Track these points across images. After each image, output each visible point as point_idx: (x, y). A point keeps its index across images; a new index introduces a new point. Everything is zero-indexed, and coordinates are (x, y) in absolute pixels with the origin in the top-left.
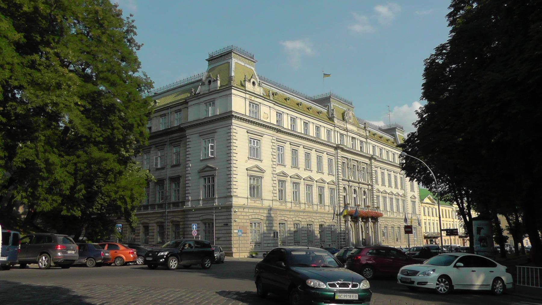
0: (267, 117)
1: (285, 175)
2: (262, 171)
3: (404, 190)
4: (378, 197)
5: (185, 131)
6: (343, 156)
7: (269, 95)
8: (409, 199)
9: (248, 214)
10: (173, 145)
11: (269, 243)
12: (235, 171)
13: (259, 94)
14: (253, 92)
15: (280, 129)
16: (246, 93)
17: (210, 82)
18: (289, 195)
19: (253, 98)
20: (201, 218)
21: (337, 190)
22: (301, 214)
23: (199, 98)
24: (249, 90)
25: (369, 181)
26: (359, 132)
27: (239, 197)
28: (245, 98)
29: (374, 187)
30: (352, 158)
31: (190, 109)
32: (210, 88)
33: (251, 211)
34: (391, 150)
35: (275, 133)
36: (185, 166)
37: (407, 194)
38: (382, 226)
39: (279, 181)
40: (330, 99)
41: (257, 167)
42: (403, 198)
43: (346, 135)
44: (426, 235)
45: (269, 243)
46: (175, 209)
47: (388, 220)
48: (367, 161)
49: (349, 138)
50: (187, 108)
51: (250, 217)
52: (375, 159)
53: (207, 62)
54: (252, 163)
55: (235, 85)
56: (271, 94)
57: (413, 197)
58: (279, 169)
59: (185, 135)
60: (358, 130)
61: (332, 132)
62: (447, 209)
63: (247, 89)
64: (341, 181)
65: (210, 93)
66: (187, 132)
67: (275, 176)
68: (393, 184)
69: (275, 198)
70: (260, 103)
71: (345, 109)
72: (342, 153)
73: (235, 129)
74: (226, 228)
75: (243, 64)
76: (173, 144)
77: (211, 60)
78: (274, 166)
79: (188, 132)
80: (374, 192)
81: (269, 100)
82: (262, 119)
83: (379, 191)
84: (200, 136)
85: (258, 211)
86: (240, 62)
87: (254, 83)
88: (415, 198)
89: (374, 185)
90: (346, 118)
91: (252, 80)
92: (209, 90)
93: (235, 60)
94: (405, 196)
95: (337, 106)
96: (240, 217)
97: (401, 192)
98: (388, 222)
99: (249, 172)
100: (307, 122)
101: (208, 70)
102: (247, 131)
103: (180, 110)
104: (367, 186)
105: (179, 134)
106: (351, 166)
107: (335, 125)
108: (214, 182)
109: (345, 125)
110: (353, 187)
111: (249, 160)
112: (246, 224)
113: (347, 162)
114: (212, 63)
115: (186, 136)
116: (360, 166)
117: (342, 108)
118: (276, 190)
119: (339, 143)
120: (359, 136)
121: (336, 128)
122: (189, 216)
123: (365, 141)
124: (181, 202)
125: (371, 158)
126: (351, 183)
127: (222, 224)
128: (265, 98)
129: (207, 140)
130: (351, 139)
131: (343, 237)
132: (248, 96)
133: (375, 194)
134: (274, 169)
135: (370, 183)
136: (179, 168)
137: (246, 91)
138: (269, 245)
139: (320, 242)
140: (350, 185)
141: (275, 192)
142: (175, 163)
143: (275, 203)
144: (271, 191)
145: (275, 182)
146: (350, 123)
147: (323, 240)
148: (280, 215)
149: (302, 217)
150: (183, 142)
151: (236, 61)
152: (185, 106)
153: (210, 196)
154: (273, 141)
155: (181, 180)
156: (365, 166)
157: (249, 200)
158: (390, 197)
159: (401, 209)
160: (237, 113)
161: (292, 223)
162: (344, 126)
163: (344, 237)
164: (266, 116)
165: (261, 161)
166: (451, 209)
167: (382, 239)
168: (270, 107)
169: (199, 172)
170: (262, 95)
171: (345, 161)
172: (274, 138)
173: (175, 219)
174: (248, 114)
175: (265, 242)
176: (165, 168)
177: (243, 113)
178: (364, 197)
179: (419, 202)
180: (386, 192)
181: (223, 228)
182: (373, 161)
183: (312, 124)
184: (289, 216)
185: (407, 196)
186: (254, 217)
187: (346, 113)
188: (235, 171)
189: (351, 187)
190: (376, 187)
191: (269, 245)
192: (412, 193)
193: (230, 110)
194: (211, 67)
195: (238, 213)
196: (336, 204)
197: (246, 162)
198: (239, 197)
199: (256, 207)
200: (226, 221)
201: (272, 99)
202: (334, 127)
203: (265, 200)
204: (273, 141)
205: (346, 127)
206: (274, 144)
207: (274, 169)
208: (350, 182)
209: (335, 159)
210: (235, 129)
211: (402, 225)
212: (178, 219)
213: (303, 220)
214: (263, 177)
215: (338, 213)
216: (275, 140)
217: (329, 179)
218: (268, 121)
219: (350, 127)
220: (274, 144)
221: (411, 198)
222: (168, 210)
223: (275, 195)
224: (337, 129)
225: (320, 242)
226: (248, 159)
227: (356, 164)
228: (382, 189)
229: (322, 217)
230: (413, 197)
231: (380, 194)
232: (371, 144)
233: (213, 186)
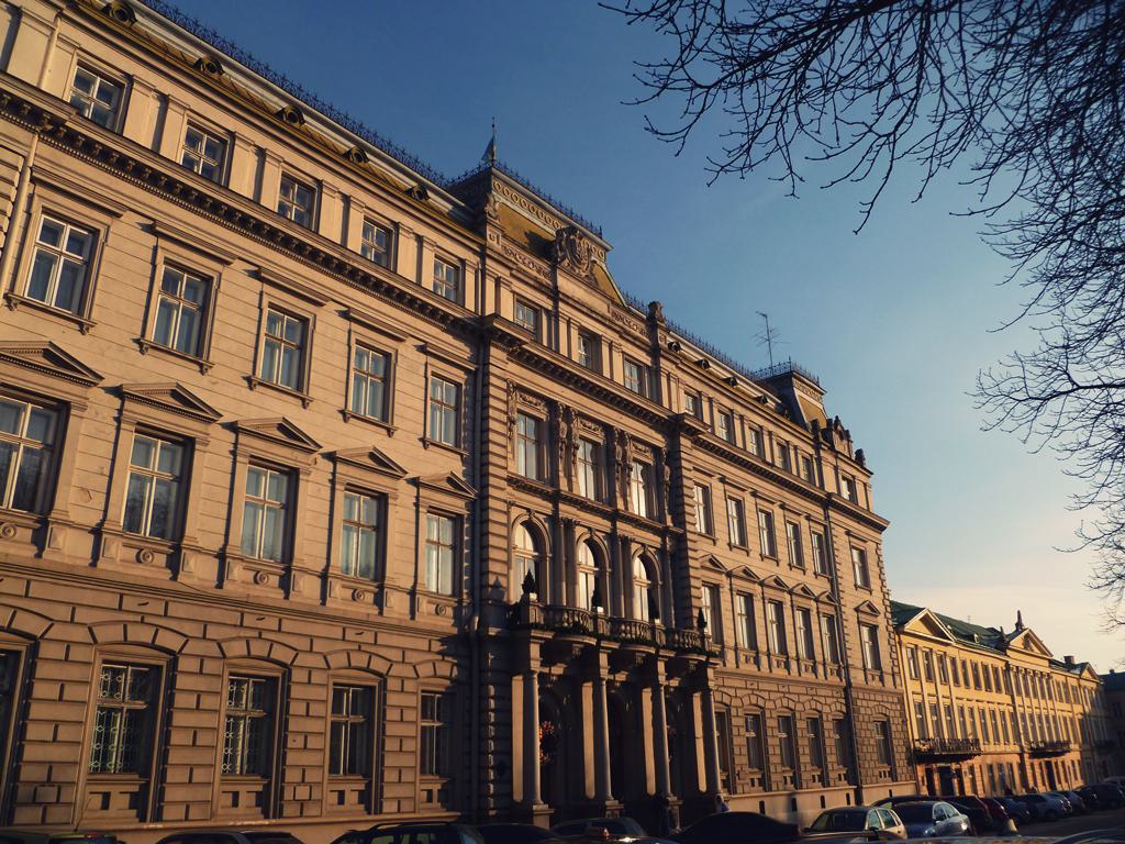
25: (669, 518)
29: (690, 544)
38: (733, 712)
40: (490, 180)
42: (830, 611)
43: (547, 311)
52: (692, 433)
62: (989, 662)
64: (503, 484)
68: (783, 551)
72: (513, 367)
80: (691, 562)
83: (715, 564)
88: (874, 611)
89: (689, 536)
95: (526, 215)
104: (659, 539)
109: (545, 275)
120: (617, 336)
121: (488, 261)
125: (673, 427)
133: (698, 574)
135: (669, 523)
146: (577, 278)
166: (1000, 665)
180: (748, 575)
190: (699, 550)
192: (863, 596)
219: (565, 284)
221: (857, 610)
228: (732, 560)
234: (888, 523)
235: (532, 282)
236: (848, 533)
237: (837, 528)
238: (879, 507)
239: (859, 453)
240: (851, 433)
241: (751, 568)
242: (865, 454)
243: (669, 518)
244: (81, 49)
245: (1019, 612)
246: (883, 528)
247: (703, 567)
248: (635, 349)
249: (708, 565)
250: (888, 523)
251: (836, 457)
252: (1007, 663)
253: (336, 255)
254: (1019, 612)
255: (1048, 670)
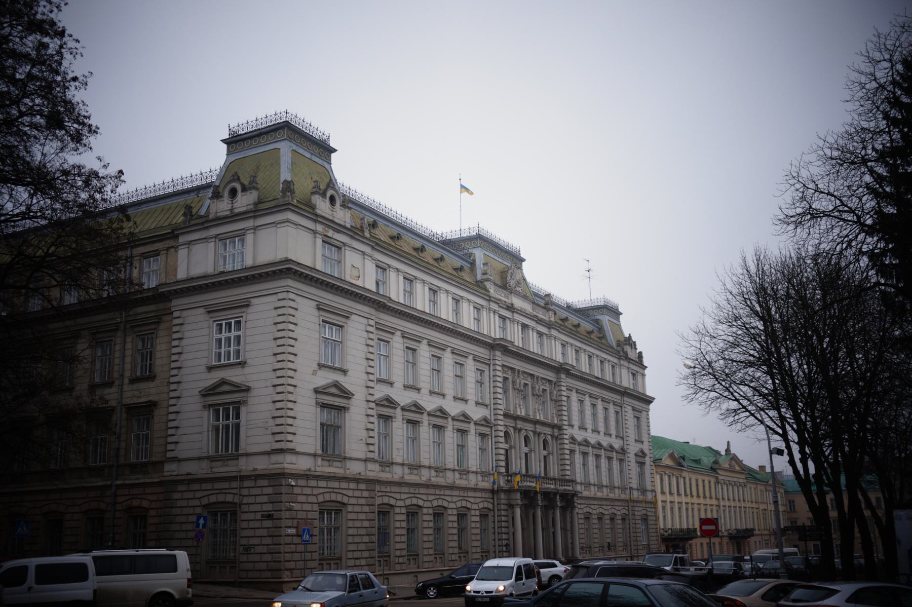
0: (357, 275)
1: (389, 402)
2: (346, 395)
3: (622, 438)
4: (572, 452)
5: (170, 301)
6: (505, 364)
7: (362, 227)
8: (632, 458)
9: (316, 491)
10: (135, 333)
11: (358, 559)
12: (292, 393)
13: (342, 223)
14: (331, 218)
15: (384, 303)
16: (316, 221)
17: (233, 193)
18: (398, 449)
19: (330, 233)
20: (205, 501)
21: (493, 439)
22: (422, 491)
23: (207, 228)
24: (324, 214)
25: (555, 419)
26: (535, 313)
27: (298, 453)
28: (314, 232)
30: (522, 369)
31: (182, 253)
32: (235, 205)
33: (322, 484)
34: (597, 352)
35: (373, 311)
36: (167, 380)
37: (628, 447)
39: (380, 416)
41: (336, 385)
42: (621, 457)
43: (509, 318)
44: (666, 534)
45: (358, 559)
46: (138, 479)
47: (592, 502)
48: (551, 376)
49: (516, 325)
50: (176, 248)
51: (321, 499)
52: (568, 373)
53: (225, 146)
54: (324, 378)
55: (295, 201)
56: (365, 226)
57: (640, 454)
58: (381, 392)
59: (170, 308)
60: (533, 310)
61: (485, 313)
63: (319, 212)
64: (501, 417)
65: (234, 217)
66: (175, 302)
67: (373, 405)
69: (370, 455)
70: (344, 244)
71: (509, 265)
73: (294, 301)
74: (268, 523)
75: (308, 155)
76: (136, 329)
77: (236, 142)
78: (371, 384)
79: (176, 303)
81: (361, 239)
82: (348, 279)
83: (573, 440)
84: (209, 312)
85: (336, 484)
86: (301, 151)
87: (332, 200)
89: (565, 427)
90: (512, 283)
91: (330, 192)
92: (231, 210)
93: (292, 145)
94: (623, 451)
95: (492, 256)
96: (301, 499)
97: (617, 444)
98: (592, 507)
99: (319, 396)
100: (436, 288)
101: (228, 163)
102: (317, 305)
103: (156, 253)
105: (152, 307)
106: (520, 386)
107: (490, 297)
108: (238, 416)
110: (523, 431)
111: (320, 369)
112: (311, 515)
113: (513, 378)
114: (236, 149)
115: (172, 313)
116: (537, 387)
117: (500, 260)
118: (373, 437)
119: (498, 337)
121: (491, 303)
122: (176, 496)
123: (547, 333)
124: (154, 464)
126: (520, 424)
127: (259, 516)
128: (356, 233)
129: (224, 323)
130: (520, 328)
131: (504, 542)
132: (320, 228)
134: (371, 391)
136: (151, 384)
137: (317, 218)
138: (358, 563)
139: (459, 553)
140: (519, 426)
141: (371, 441)
142: (139, 374)
143: (371, 466)
144: (364, 439)
145: (372, 419)
146: (518, 294)
147: (463, 548)
148: (380, 494)
149: (424, 497)
150: (162, 326)
151: (295, 147)
152: (171, 243)
153: (227, 450)
154: (370, 329)
155: (159, 413)
156: (547, 387)
157: (319, 460)
158: (594, 453)
159: (616, 480)
160: (299, 264)
161: (404, 510)
162: (506, 300)
163: (507, 541)
164: (355, 273)
165: (345, 372)
167: (581, 545)
168: (364, 253)
169: (204, 396)
170: (348, 226)
171: (509, 375)
172: (372, 323)
173: (135, 503)
174: (319, 267)
175: (350, 555)
176: (113, 383)
177: (309, 264)
178: (545, 453)
179: (652, 463)
181: (258, 524)
182: (563, 376)
183: (445, 295)
184: (399, 495)
185: (628, 451)
186: (327, 497)
187: (510, 271)
188: (292, 393)
189: (520, 430)
190: (568, 431)
191: (358, 563)
192: (639, 446)
193: (285, 256)
194: (233, 158)
195: (297, 490)
196: (491, 469)
197: (314, 373)
198: (298, 453)
199: (333, 475)
200: (268, 507)
201: (367, 234)
202: (489, 301)
203: (351, 459)
204: (370, 329)
205: (509, 301)
206: (371, 336)
207: (371, 391)
208: (518, 422)
209: (489, 370)
210: (294, 301)
211: (619, 513)
212: (145, 504)
213: (427, 504)
214: (348, 409)
215: (496, 489)
216: (373, 326)
217: (477, 413)
218: (359, 283)
220: (371, 336)
221: (636, 455)
222: (119, 482)
223: (371, 448)
224: (494, 306)
225: (459, 553)
226: (317, 366)
227: (529, 381)
228: (579, 436)
229: (464, 498)
230: (640, 454)
231: (577, 448)
232: (559, 339)
233: (237, 427)
234: (654, 399)
235: (505, 307)
236: (634, 409)
237: (628, 407)
238: (649, 392)
239: (640, 353)
240: (637, 344)
241: (588, 439)
242: (644, 355)
243: (555, 419)
244: (378, 260)
245: (728, 442)
246: (651, 402)
247: (570, 443)
248: (543, 328)
249: (571, 440)
250: (654, 399)
251: (629, 362)
252: (717, 477)
253: (451, 327)
254: (728, 442)
255: (744, 481)
